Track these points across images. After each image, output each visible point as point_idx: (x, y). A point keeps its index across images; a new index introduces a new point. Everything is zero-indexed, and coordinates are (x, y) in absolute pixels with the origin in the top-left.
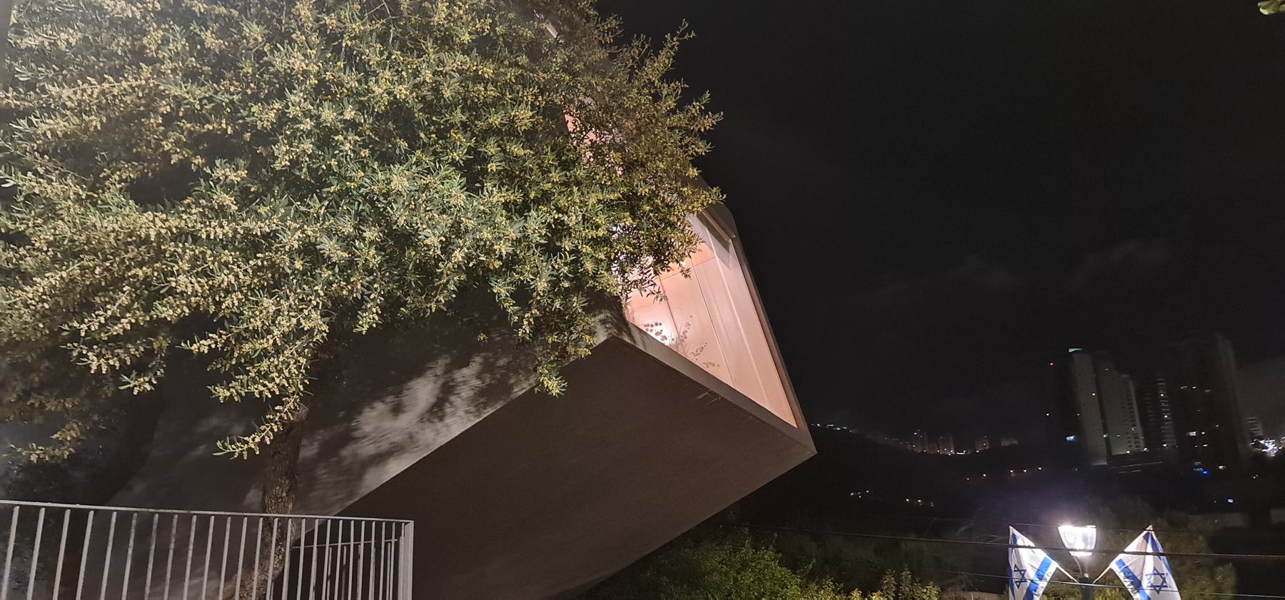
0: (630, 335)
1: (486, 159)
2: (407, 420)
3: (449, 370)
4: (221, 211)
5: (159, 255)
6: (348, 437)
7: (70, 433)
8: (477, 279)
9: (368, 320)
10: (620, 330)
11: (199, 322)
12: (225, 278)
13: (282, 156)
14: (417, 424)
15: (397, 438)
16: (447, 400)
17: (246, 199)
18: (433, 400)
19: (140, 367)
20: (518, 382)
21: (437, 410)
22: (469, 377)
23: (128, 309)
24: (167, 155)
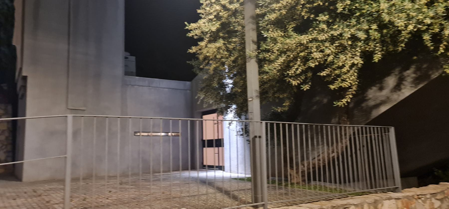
2: (385, 92)
3: (401, 72)
4: (323, 30)
5: (307, 48)
7: (287, 104)
8: (417, 36)
9: (377, 57)
11: (322, 66)
12: (327, 51)
14: (391, 93)
15: (383, 99)
16: (402, 84)
17: (329, 24)
18: (395, 84)
20: (433, 73)
21: (398, 87)
22: (410, 74)
23: (299, 66)
24: (303, 16)
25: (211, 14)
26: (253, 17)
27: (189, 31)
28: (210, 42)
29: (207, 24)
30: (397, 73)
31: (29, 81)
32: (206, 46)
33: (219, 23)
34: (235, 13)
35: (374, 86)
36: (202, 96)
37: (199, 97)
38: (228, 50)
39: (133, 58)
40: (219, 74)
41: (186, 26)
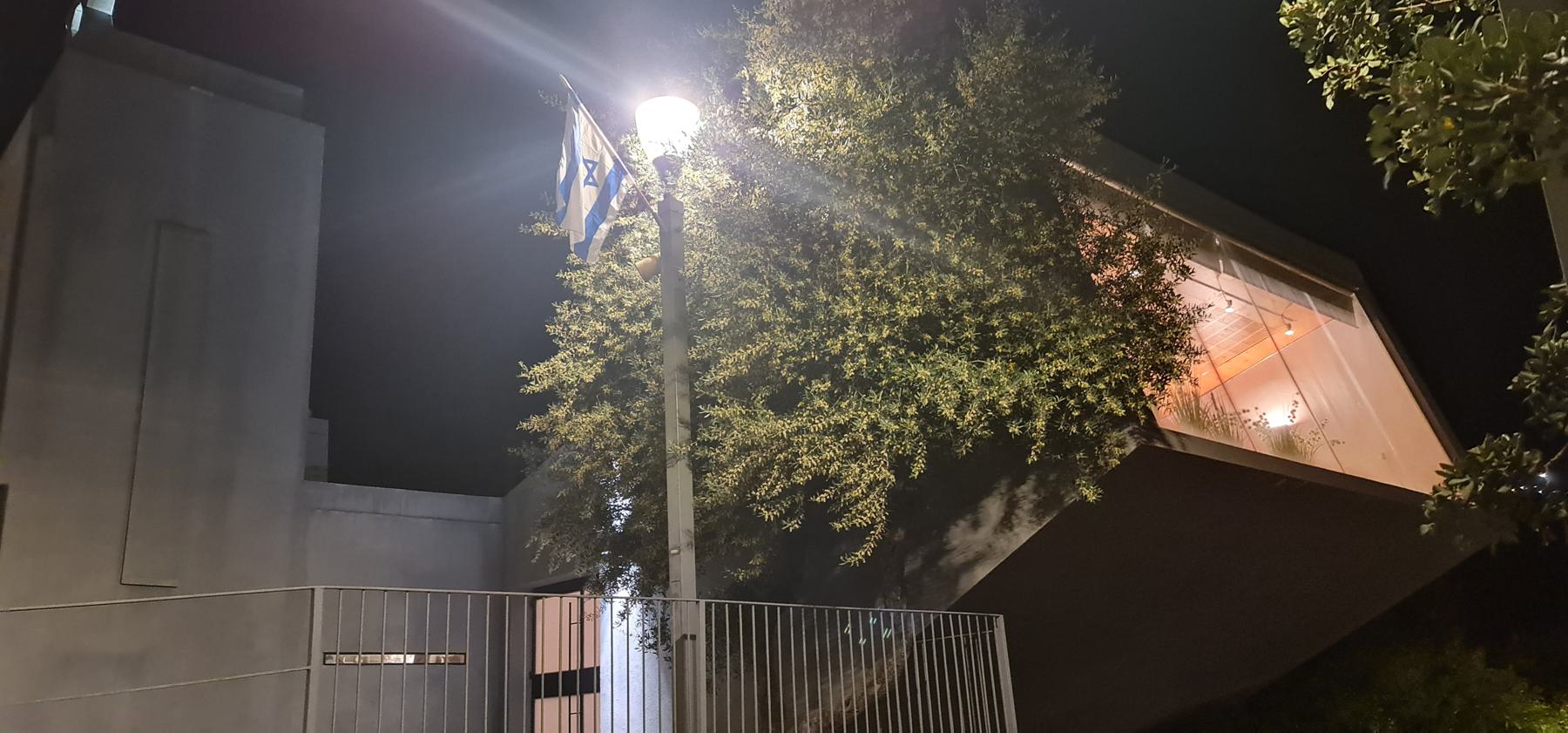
0: (1165, 441)
1: (994, 329)
2: (984, 533)
5: (790, 444)
6: (943, 551)
7: (757, 560)
9: (918, 468)
10: (1150, 438)
11: (820, 482)
12: (828, 454)
13: (849, 369)
14: (993, 536)
15: (979, 548)
17: (832, 398)
19: (790, 514)
21: (1006, 523)
23: (778, 479)
24: (785, 379)
25: (583, 340)
26: (682, 369)
27: (527, 382)
28: (577, 407)
29: (571, 364)
30: (1003, 490)
31: (11, 497)
32: (568, 418)
33: (601, 362)
34: (640, 345)
35: (962, 517)
36: (545, 542)
37: (536, 545)
38: (621, 427)
39: (324, 425)
40: (597, 490)
41: (520, 370)
